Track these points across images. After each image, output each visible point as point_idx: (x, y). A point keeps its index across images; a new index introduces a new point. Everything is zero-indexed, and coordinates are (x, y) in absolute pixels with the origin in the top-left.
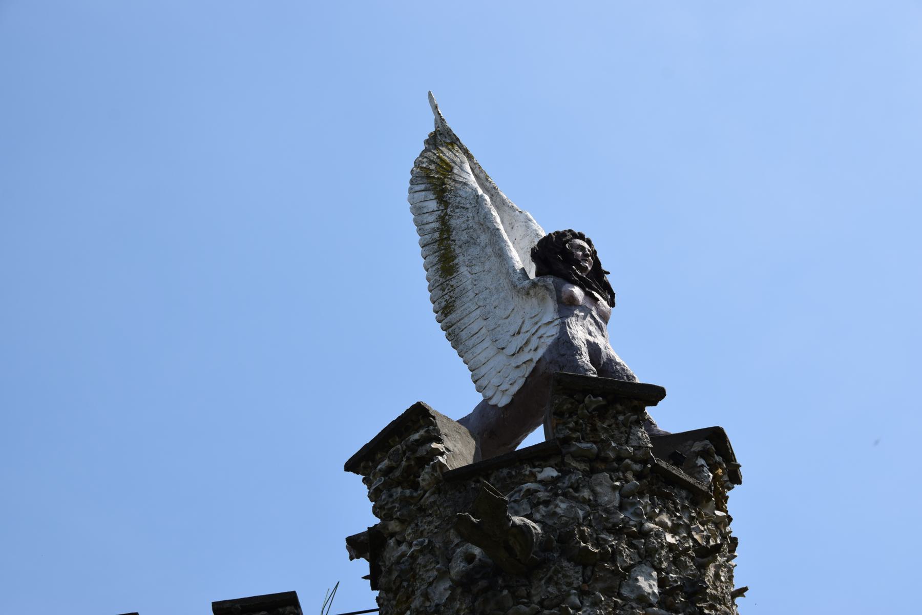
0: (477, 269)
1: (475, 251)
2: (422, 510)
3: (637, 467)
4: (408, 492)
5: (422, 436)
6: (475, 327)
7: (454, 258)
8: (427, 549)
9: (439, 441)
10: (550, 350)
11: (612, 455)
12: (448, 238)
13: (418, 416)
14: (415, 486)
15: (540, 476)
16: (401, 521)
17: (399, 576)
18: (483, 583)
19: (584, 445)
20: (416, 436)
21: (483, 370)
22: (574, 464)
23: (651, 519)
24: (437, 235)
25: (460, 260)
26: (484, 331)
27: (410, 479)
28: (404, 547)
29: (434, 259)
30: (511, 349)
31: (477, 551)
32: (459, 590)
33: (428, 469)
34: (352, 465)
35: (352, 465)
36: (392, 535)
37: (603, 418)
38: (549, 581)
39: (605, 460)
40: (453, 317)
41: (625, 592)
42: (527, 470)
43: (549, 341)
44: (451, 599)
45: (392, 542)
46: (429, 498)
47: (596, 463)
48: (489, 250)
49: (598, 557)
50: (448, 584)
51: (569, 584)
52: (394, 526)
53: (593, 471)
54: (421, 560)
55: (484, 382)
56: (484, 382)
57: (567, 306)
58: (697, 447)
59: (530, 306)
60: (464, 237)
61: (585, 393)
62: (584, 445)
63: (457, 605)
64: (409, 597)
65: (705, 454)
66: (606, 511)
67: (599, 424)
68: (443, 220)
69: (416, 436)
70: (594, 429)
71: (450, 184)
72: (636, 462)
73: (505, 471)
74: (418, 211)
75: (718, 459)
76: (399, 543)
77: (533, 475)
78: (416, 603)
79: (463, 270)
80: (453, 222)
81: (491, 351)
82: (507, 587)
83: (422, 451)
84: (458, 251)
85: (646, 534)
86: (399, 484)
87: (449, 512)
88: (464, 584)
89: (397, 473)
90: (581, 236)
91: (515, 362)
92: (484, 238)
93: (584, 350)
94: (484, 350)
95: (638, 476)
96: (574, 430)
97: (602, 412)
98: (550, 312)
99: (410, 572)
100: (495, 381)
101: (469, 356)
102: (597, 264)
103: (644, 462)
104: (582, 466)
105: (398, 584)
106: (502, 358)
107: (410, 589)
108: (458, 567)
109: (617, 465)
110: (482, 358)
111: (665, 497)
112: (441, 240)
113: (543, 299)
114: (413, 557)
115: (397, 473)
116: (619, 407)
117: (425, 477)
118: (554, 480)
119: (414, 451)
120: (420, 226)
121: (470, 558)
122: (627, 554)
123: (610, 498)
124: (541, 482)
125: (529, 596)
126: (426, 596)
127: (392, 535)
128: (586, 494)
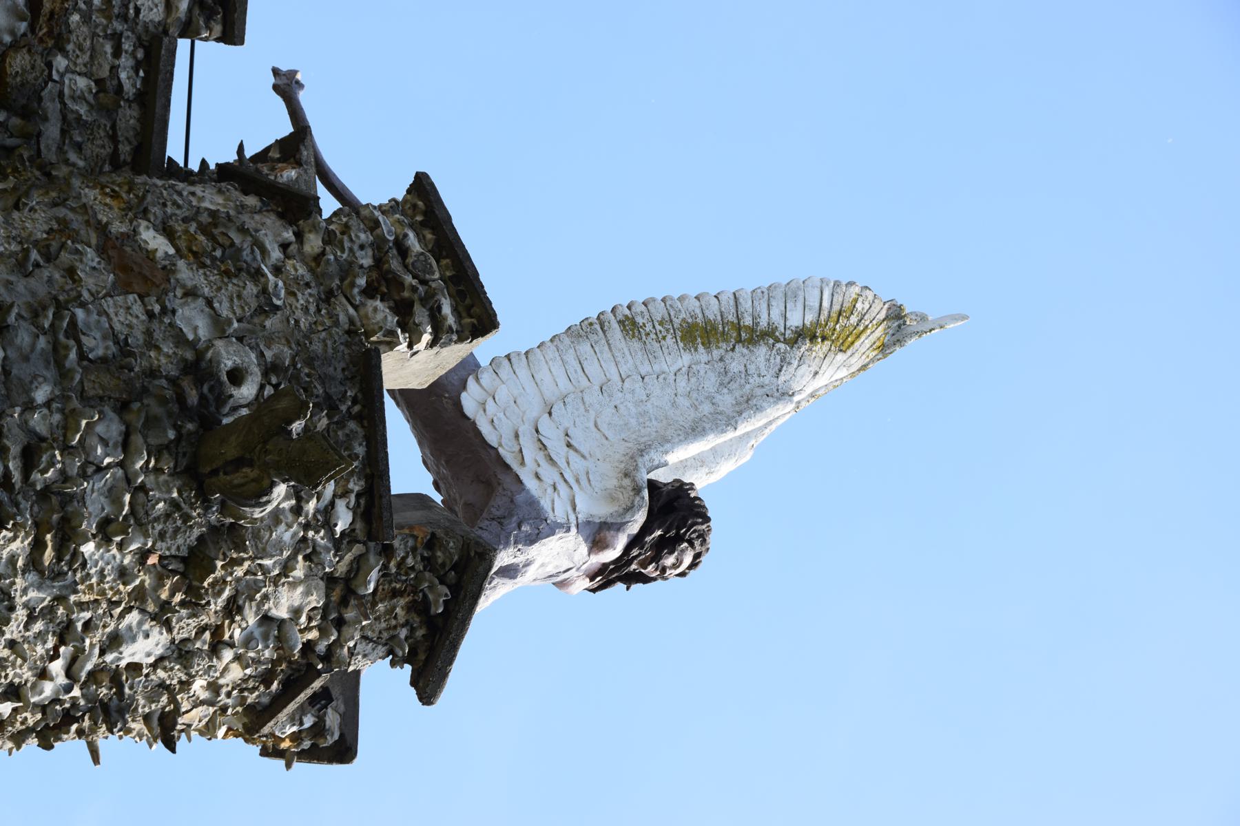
0: (682, 382)
1: (711, 382)
2: (328, 297)
3: (321, 647)
4: (362, 281)
5: (445, 319)
6: (592, 368)
7: (707, 345)
8: (267, 307)
9: (432, 344)
10: (533, 503)
11: (350, 614)
12: (739, 340)
13: (479, 319)
14: (370, 292)
15: (341, 505)
16: (319, 257)
17: (233, 244)
18: (193, 397)
19: (374, 575)
20: (447, 309)
21: (523, 372)
22: (348, 557)
23: (237, 658)
24: (748, 321)
25: (702, 354)
26: (585, 382)
27: (383, 284)
28: (276, 254)
29: (713, 313)
30: (546, 426)
31: (247, 391)
32: (189, 355)
33: (392, 320)
34: (422, 186)
35: (422, 186)
36: (299, 236)
37: (409, 608)
38: (174, 505)
39: (344, 602)
40: (616, 331)
41: (134, 617)
42: (355, 486)
43: (545, 503)
44: (179, 338)
45: (289, 235)
46: (344, 312)
47: (342, 592)
48: (706, 408)
49: (196, 583)
50: (203, 333)
51: (162, 536)
52: (313, 243)
53: (330, 580)
54: (251, 289)
55: (505, 370)
56: (505, 370)
57: (597, 537)
58: (332, 719)
59: (607, 476)
60: (735, 367)
61: (455, 589)
62: (374, 575)
63: (167, 348)
64: (198, 259)
65: (319, 729)
66: (266, 597)
67: (402, 601)
68: (769, 334)
69: (447, 309)
70: (395, 594)
71: (821, 348)
72: (329, 647)
73: (360, 450)
74: (791, 293)
75: (307, 744)
76: (284, 246)
77: (345, 494)
78: (185, 273)
79: (686, 358)
80: (762, 351)
81: (550, 392)
82: (179, 438)
83: (421, 315)
84: (716, 353)
85: (215, 649)
86: (379, 262)
87: (317, 347)
88: (198, 367)
89: (395, 264)
90: (693, 565)
91: (526, 430)
92: (726, 401)
93: (521, 559)
94: (553, 376)
95: (309, 646)
96: (399, 565)
97: (420, 607)
98: (591, 507)
99: (234, 266)
100: (503, 394)
101: (551, 352)
102: (646, 580)
103: (328, 657)
104: (342, 569)
105: (220, 239)
106: (533, 408)
107: (208, 262)
108: (228, 356)
109: (332, 617)
110: (543, 375)
111: (266, 679)
112: (738, 327)
113: (612, 498)
114: (257, 275)
115: (395, 264)
116: (420, 633)
117: (380, 312)
118: (329, 525)
119: (423, 301)
120: (768, 293)
121: (237, 376)
122: (185, 626)
123: (283, 603)
124: (332, 504)
125: (158, 470)
126: (192, 293)
127: (299, 236)
128: (299, 572)
